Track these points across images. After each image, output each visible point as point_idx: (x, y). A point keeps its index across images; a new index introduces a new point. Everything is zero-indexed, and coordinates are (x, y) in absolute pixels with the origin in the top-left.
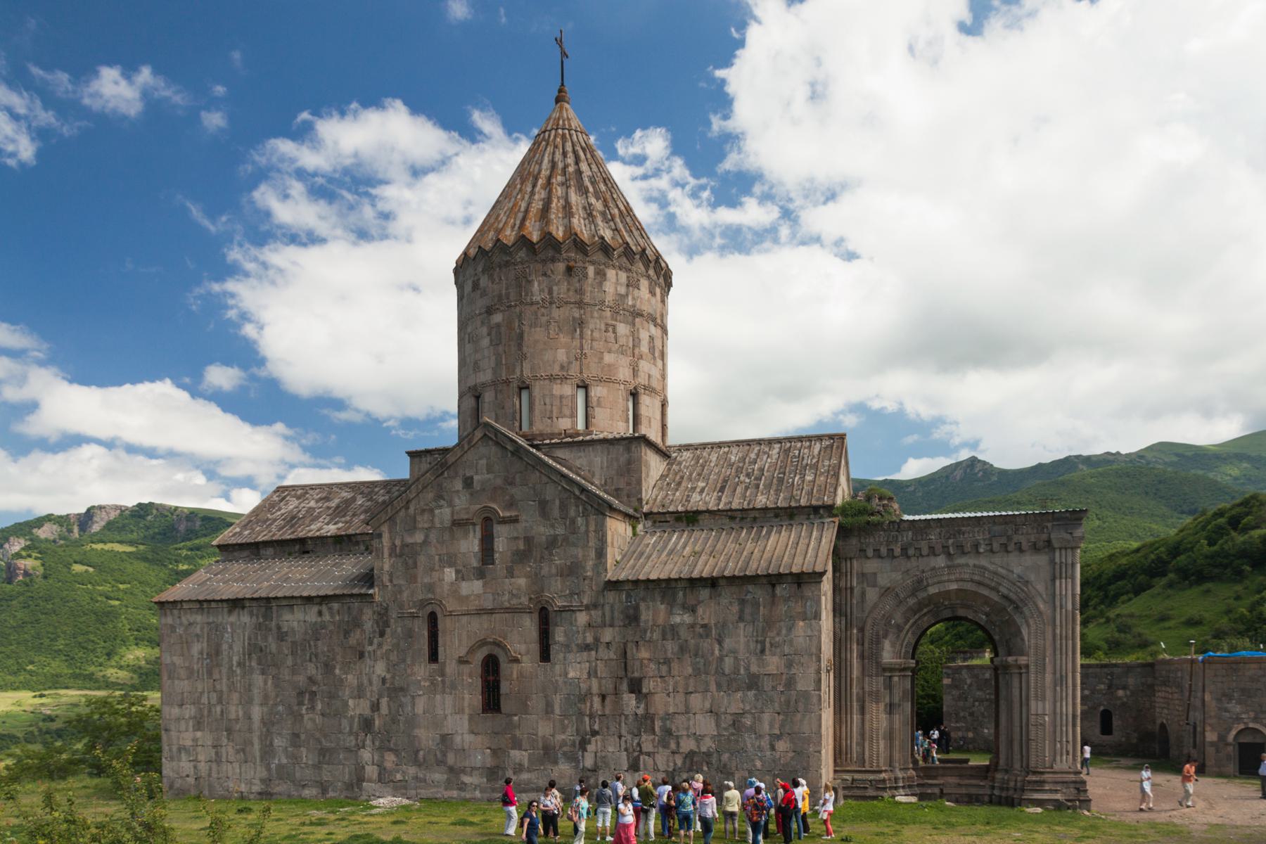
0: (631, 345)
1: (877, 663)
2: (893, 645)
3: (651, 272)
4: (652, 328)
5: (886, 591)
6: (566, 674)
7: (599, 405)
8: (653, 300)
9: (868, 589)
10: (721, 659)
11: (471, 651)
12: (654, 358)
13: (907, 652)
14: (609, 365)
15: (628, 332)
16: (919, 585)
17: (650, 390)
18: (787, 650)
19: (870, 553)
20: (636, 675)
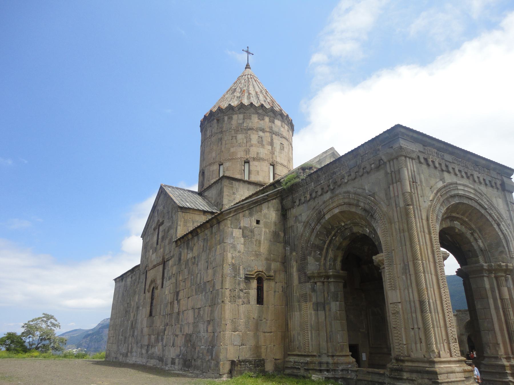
0: (245, 142)
1: (305, 273)
2: (318, 260)
3: (260, 111)
4: (261, 134)
5: (307, 224)
6: (165, 292)
7: (227, 170)
8: (262, 122)
9: (299, 225)
10: (197, 275)
11: (150, 286)
12: (263, 146)
13: (330, 264)
14: (233, 153)
15: (243, 137)
16: (320, 216)
17: (258, 159)
18: (214, 264)
19: (297, 203)
20: (178, 290)
